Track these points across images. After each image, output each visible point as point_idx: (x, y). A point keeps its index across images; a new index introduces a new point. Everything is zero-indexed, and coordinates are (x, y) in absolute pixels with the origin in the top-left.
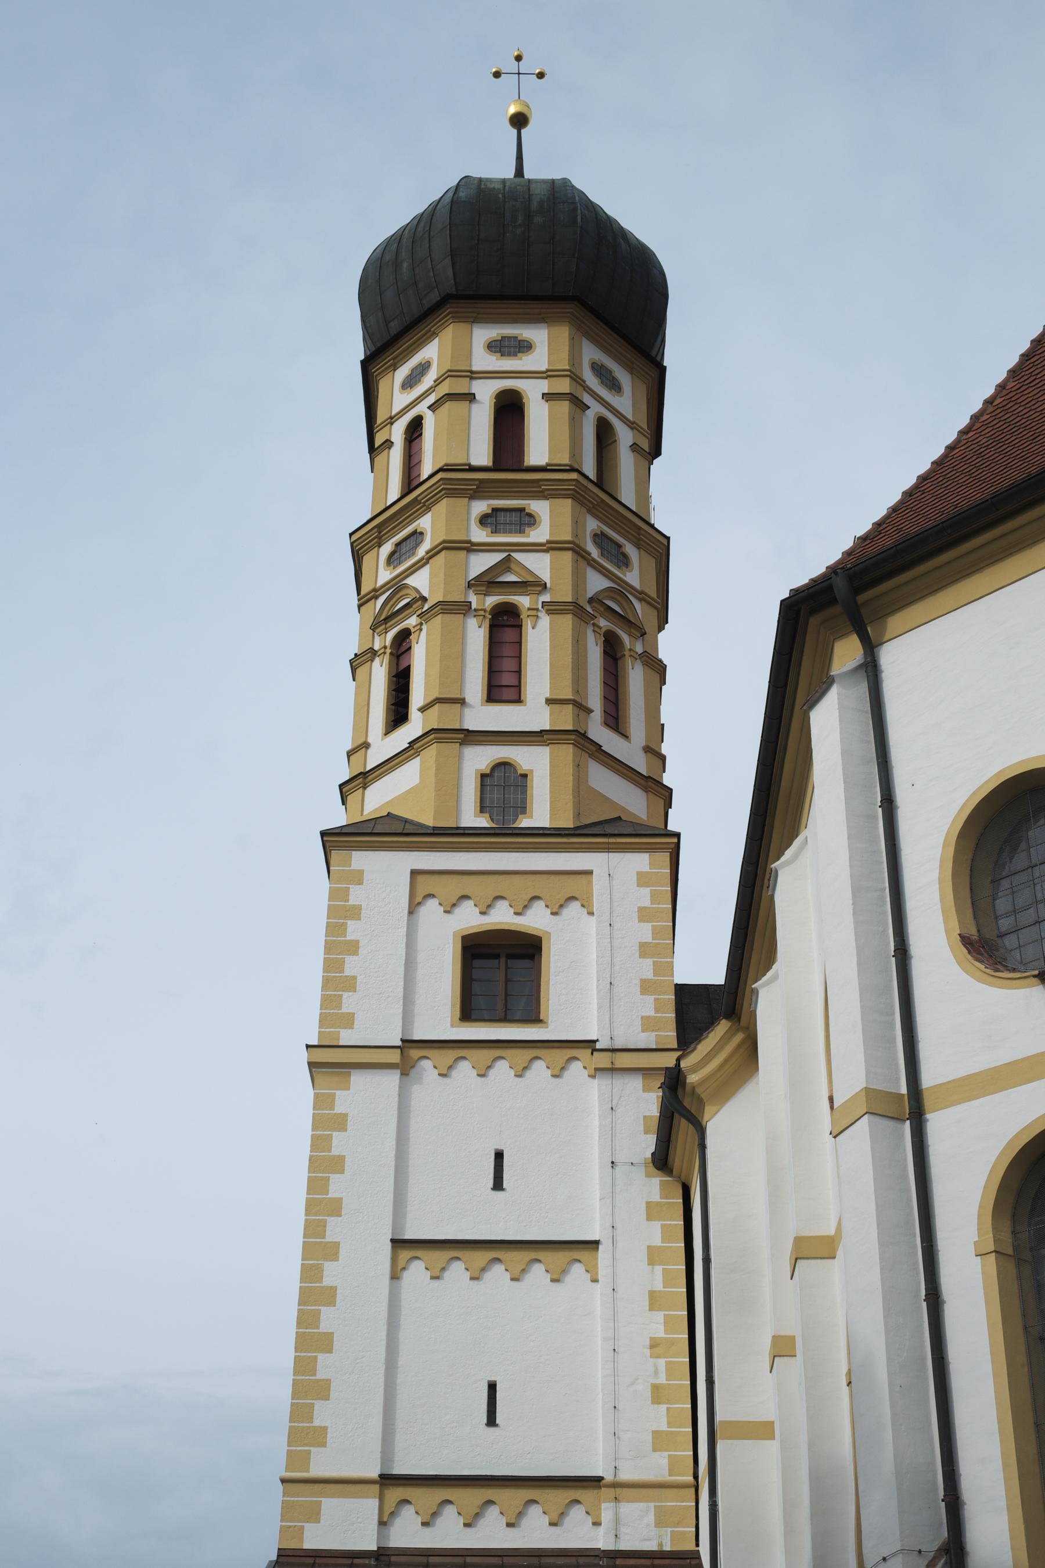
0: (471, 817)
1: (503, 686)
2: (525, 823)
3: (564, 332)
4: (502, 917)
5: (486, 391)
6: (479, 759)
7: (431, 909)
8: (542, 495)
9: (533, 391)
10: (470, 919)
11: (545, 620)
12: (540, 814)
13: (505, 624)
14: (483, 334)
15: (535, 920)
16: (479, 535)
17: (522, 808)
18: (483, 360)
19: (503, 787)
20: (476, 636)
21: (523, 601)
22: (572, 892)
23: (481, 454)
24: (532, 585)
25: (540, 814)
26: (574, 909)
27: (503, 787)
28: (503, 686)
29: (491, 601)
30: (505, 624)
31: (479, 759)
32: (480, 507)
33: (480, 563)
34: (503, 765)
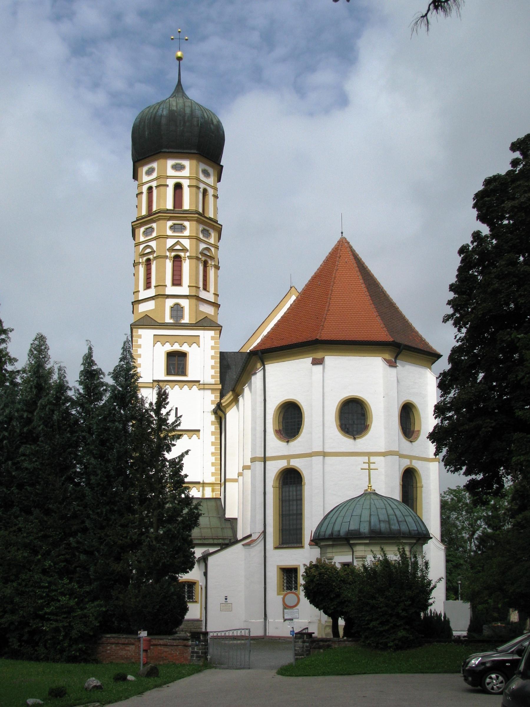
0: (168, 319)
1: (177, 282)
3: (194, 162)
5: (171, 183)
6: (170, 303)
8: (188, 220)
9: (186, 183)
10: (168, 348)
11: (188, 261)
12: (186, 320)
13: (177, 260)
14: (170, 163)
15: (185, 348)
16: (169, 233)
17: (182, 317)
18: (170, 172)
19: (177, 310)
20: (169, 265)
21: (182, 254)
22: (195, 340)
25: (186, 320)
27: (177, 310)
28: (177, 282)
29: (173, 254)
30: (177, 260)
31: (170, 303)
32: (170, 223)
33: (170, 242)
34: (177, 304)
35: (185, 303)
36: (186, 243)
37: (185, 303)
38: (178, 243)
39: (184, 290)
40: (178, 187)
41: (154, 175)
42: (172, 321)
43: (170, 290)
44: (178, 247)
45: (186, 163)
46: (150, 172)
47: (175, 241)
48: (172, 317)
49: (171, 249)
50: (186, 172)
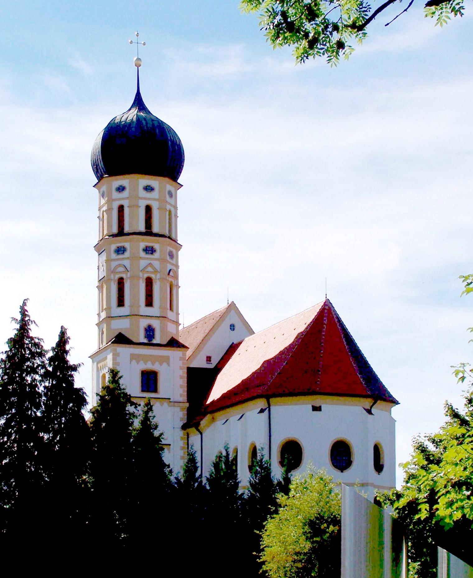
1: (149, 302)
2: (154, 341)
4: (149, 366)
5: (142, 205)
7: (134, 362)
13: (149, 282)
15: (155, 367)
16: (143, 254)
18: (142, 193)
19: (150, 332)
22: (166, 360)
23: (142, 228)
24: (156, 271)
26: (165, 364)
27: (150, 332)
30: (149, 282)
31: (144, 323)
33: (143, 263)
36: (157, 264)
37: (155, 324)
40: (148, 209)
41: (126, 194)
42: (146, 341)
44: (150, 269)
46: (121, 189)
50: (155, 194)
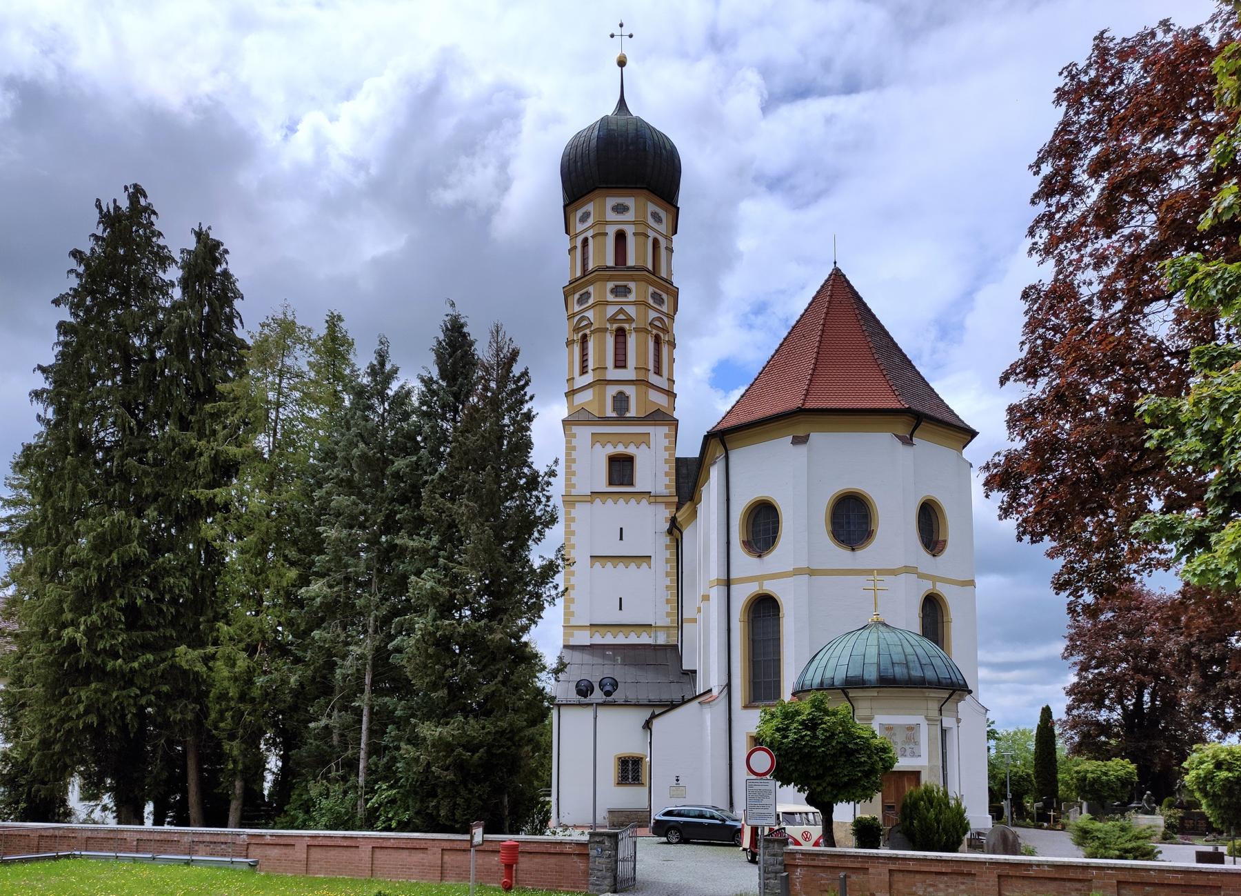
0: (610, 413)
1: (620, 363)
5: (611, 231)
6: (612, 391)
9: (630, 230)
10: (611, 450)
12: (632, 413)
13: (621, 334)
14: (611, 202)
15: (631, 450)
16: (610, 298)
17: (627, 410)
18: (611, 216)
19: (621, 401)
20: (610, 340)
22: (644, 439)
25: (632, 413)
27: (621, 401)
28: (620, 363)
29: (615, 326)
30: (621, 334)
31: (612, 391)
32: (610, 285)
33: (611, 311)
34: (621, 393)
35: (630, 391)
36: (631, 311)
37: (630, 391)
38: (621, 311)
39: (629, 374)
40: (621, 237)
42: (614, 415)
43: (613, 374)
44: (621, 317)
45: (630, 202)
47: (617, 308)
48: (614, 410)
49: (613, 320)
50: (630, 216)
